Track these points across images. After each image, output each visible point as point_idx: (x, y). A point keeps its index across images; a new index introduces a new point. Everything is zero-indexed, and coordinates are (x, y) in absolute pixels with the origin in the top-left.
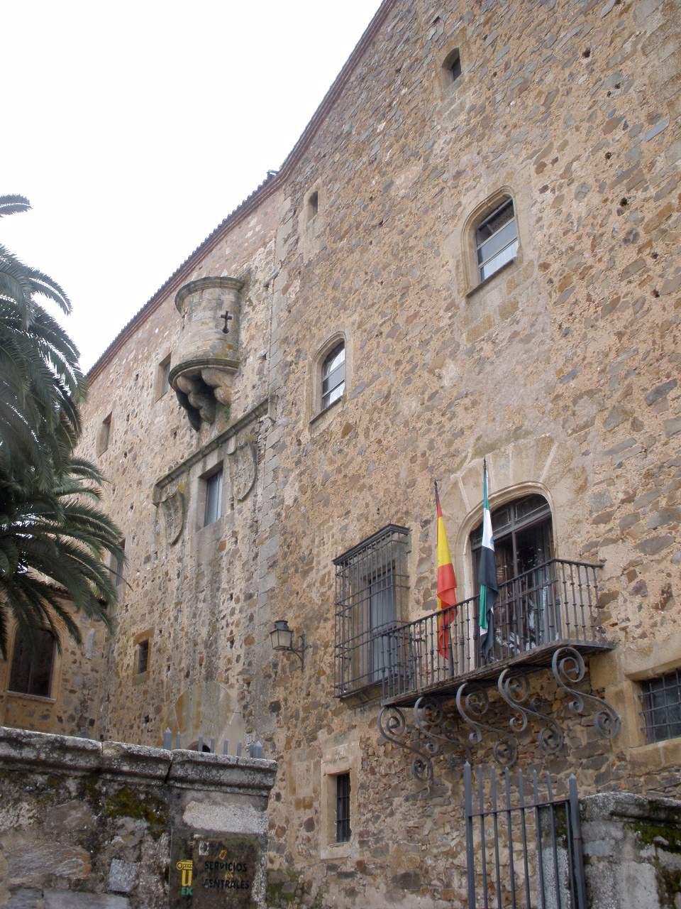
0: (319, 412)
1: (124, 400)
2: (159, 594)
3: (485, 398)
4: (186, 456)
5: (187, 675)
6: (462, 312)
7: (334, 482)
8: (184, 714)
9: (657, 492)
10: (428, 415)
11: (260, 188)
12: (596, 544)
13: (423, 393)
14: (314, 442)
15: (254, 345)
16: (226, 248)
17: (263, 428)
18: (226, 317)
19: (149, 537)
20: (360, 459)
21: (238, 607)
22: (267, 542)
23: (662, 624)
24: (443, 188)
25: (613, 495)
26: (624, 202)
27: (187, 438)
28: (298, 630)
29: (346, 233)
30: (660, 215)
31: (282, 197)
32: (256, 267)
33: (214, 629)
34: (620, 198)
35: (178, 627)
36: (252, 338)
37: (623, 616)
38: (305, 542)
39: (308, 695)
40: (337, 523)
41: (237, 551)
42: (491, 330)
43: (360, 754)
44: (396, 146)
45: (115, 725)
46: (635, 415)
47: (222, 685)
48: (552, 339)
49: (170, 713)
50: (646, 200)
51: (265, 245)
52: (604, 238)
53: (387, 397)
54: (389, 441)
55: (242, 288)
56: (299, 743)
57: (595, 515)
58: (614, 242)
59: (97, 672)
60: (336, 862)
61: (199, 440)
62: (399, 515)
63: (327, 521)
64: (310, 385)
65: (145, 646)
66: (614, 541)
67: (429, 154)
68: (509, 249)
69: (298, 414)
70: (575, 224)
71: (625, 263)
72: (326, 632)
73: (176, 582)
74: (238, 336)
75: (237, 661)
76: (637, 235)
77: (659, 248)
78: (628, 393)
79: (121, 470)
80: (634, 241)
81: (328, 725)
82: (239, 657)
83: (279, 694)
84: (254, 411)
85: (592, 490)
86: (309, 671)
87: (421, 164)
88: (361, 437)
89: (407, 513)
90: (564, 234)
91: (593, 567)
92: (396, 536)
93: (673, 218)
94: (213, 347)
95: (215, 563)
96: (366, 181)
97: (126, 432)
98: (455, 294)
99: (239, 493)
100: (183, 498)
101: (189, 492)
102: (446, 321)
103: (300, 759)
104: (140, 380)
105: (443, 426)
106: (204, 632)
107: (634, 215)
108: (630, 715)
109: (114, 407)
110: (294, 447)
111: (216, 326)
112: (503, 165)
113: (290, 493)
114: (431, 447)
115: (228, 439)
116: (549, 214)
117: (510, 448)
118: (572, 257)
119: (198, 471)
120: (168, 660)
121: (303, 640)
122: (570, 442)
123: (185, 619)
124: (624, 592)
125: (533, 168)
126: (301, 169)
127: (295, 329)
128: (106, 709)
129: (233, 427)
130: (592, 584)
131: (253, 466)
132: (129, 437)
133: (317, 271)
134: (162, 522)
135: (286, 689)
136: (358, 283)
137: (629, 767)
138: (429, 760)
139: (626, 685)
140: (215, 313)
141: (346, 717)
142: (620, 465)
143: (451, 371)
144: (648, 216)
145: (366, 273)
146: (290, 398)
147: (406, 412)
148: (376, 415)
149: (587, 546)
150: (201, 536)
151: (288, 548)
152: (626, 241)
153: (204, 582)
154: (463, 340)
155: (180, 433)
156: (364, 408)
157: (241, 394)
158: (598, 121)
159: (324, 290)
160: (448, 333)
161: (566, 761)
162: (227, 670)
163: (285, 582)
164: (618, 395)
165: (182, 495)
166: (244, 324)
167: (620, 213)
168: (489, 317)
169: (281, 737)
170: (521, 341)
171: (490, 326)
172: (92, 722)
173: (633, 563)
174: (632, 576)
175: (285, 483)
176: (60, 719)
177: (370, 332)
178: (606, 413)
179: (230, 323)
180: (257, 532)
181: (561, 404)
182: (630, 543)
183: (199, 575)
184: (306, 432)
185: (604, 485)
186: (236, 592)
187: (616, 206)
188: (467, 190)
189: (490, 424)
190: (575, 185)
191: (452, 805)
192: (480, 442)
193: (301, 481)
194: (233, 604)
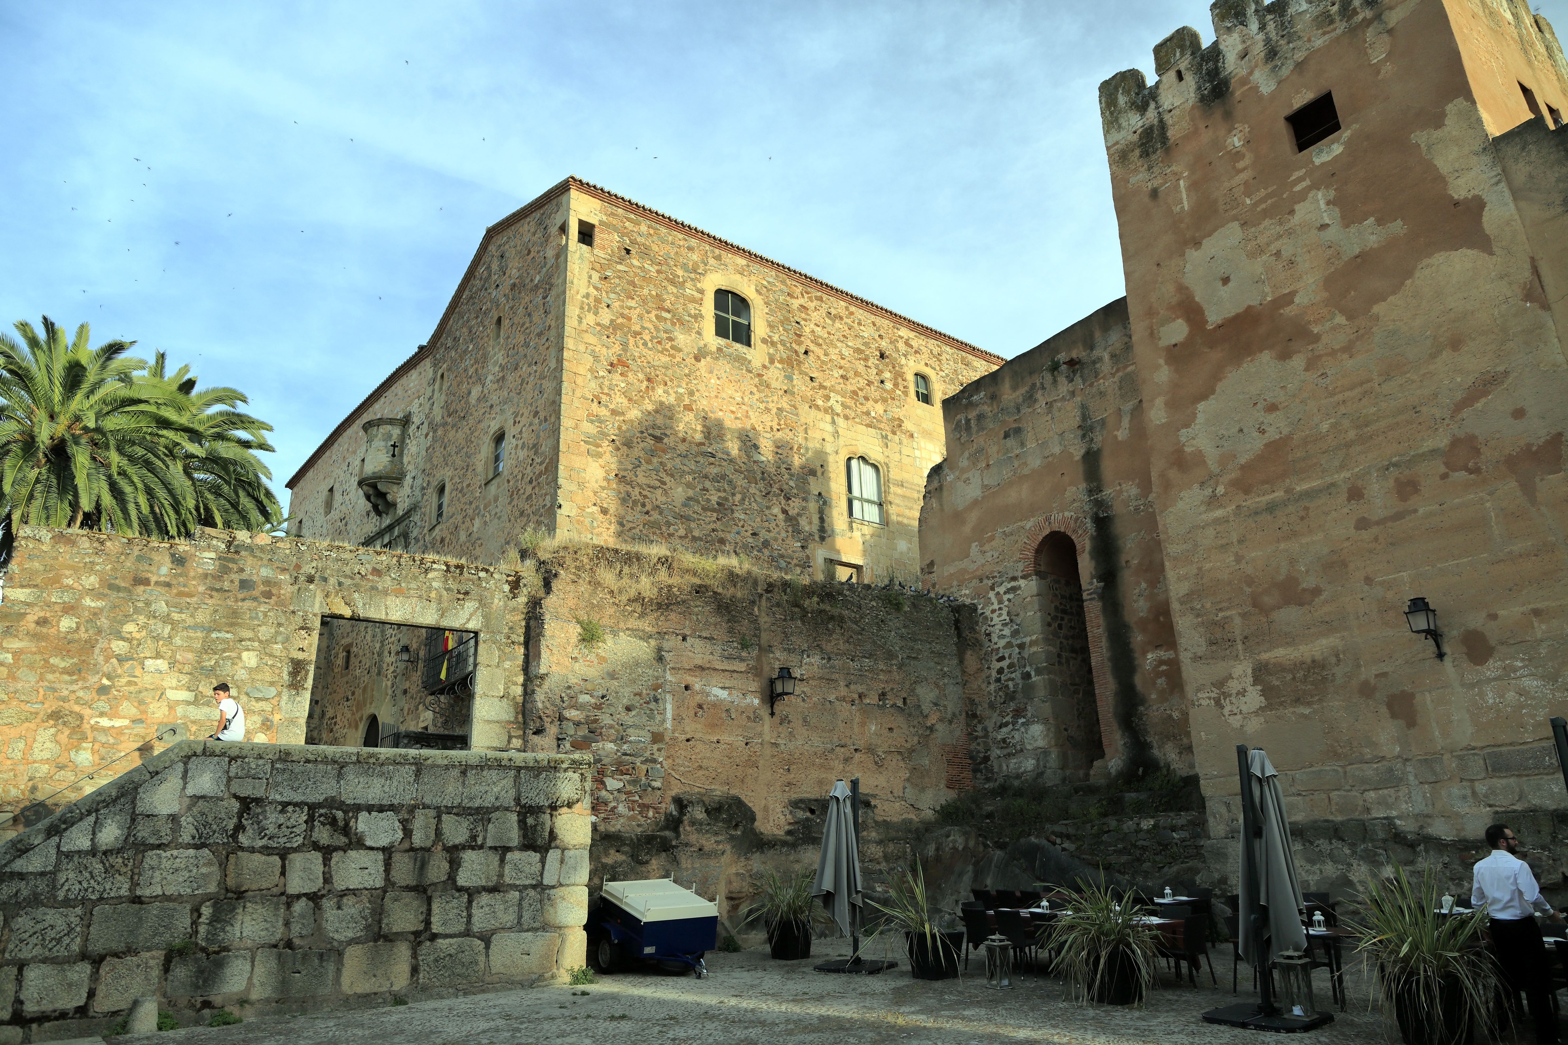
18: (394, 446)
65: (348, 652)
94: (385, 467)
106: (378, 645)
110: (422, 542)
123: (369, 638)
179: (397, 449)
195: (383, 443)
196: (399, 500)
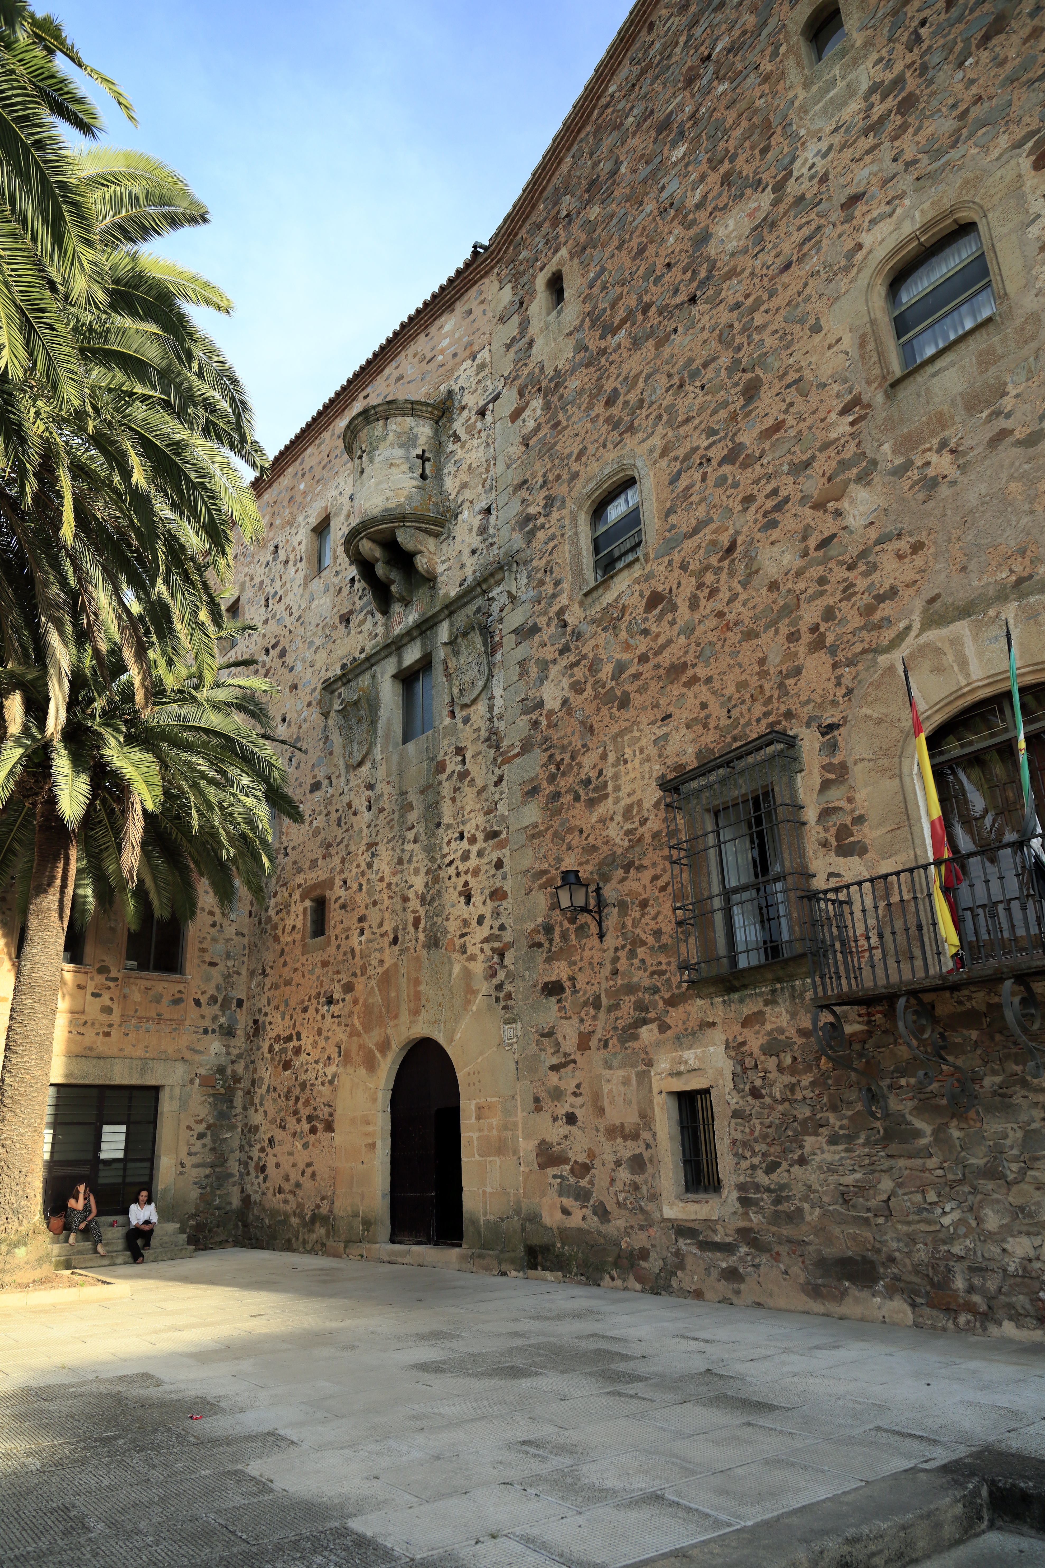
1: (257, 580)
5: (395, 941)
8: (393, 994)
13: (804, 539)
15: (468, 494)
18: (422, 457)
21: (474, 849)
22: (517, 760)
38: (588, 761)
40: (647, 734)
41: (464, 775)
47: (456, 956)
61: (387, 626)
64: (575, 541)
73: (366, 817)
86: (611, 941)
88: (683, 609)
94: (409, 498)
95: (430, 789)
100: (372, 704)
104: (282, 553)
106: (419, 882)
111: (411, 470)
113: (552, 694)
145: (669, 376)
155: (355, 620)
157: (451, 562)
162: (462, 935)
166: (450, 468)
180: (498, 747)
186: (469, 829)
188: (873, 222)
194: (465, 845)
195: (399, 452)
196: (440, 569)
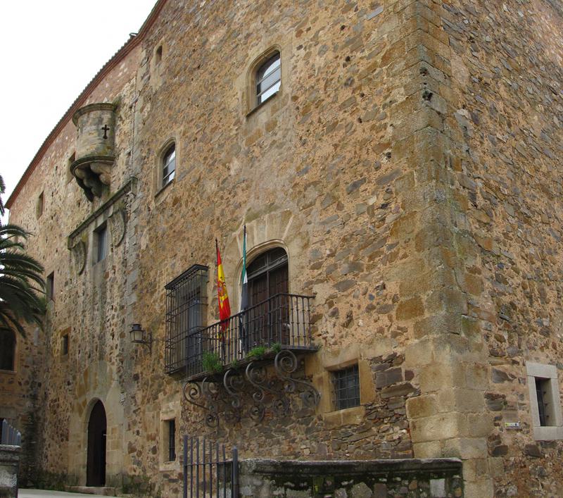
0: (161, 188)
1: (50, 183)
2: (73, 305)
3: (254, 183)
4: (86, 218)
5: (89, 357)
6: (243, 126)
7: (168, 236)
8: (88, 380)
9: (349, 251)
10: (221, 193)
11: (126, 44)
12: (311, 283)
13: (219, 179)
14: (157, 209)
15: (124, 146)
16: (105, 84)
17: (129, 199)
18: (105, 129)
19: (67, 270)
20: (183, 220)
21: (116, 314)
22: (132, 273)
23: (346, 337)
24: (238, 45)
25: (323, 251)
26: (348, 59)
27: (86, 207)
28: (148, 329)
29: (178, 73)
30: (368, 69)
31: (141, 49)
32: (125, 96)
33: (103, 328)
34: (346, 56)
35: (85, 326)
36: (122, 141)
37: (324, 330)
38: (152, 274)
39: (154, 370)
40: (170, 262)
41: (115, 278)
42: (259, 139)
43: (180, 408)
44: (211, 17)
45: (52, 386)
46: (340, 200)
47: (108, 363)
48: (296, 147)
49: (81, 380)
50: (361, 58)
51: (129, 81)
52: (333, 82)
53: (198, 181)
54: (199, 209)
55: (115, 109)
56: (148, 400)
57: (312, 263)
58: (339, 85)
59: (41, 354)
60: (168, 473)
61: (93, 207)
62: (203, 258)
63: (164, 260)
64: (155, 172)
65: (66, 338)
66: (322, 281)
67: (231, 22)
68: (273, 88)
69: (148, 191)
70: (316, 71)
71: (344, 99)
72: (162, 331)
73: (82, 298)
74: (114, 140)
75: (116, 348)
76: (353, 81)
77: (365, 91)
78: (337, 185)
79: (50, 227)
80: (351, 85)
81: (164, 390)
82: (117, 345)
83: (138, 370)
84: (123, 189)
85: (312, 247)
86: (154, 356)
87: (226, 28)
88: (184, 206)
89: (208, 256)
90: (309, 78)
91: (308, 298)
92: (200, 272)
93: (377, 72)
94: (97, 149)
95: (103, 286)
96: (192, 39)
97: (52, 204)
98: (240, 114)
99: (115, 241)
100: (85, 245)
101: (88, 241)
102: (234, 132)
103: (149, 411)
104: (58, 170)
105: (230, 201)
106: (98, 329)
107: (352, 68)
108: (325, 393)
109: (45, 187)
110: (146, 212)
111: (99, 135)
112: (276, 30)
113: (144, 242)
114: (222, 215)
115: (110, 206)
116: (301, 64)
117: (266, 217)
118: (312, 93)
119: (92, 227)
120: (79, 347)
121: (151, 335)
122: (301, 215)
123: (87, 322)
124: (326, 315)
125: (294, 33)
126: (152, 31)
127: (147, 136)
128: (47, 377)
129: (112, 199)
130: (307, 309)
131: (123, 225)
132: (54, 206)
133: (161, 98)
134: (74, 260)
135: (142, 366)
136: (184, 106)
137: (324, 425)
138: (217, 414)
139: (324, 374)
140: (98, 127)
141: (173, 385)
142: (329, 232)
143: (235, 164)
144: (362, 69)
145: (189, 99)
146: (144, 180)
147: (209, 191)
148: (192, 192)
149: (306, 283)
150: (95, 269)
151: (143, 276)
152: (346, 84)
153: (97, 298)
154: (243, 144)
155: (82, 203)
156: (185, 187)
157: (117, 177)
158: (339, 5)
159: (164, 110)
160: (235, 141)
161: (290, 419)
162: (111, 353)
163: (142, 298)
164: (330, 186)
165: (84, 244)
166: (118, 133)
167: (345, 65)
168: (259, 130)
169: (139, 396)
170: (277, 146)
171: (260, 136)
172: (40, 385)
173: (332, 297)
174: (331, 305)
175: (141, 235)
176: (20, 383)
177: (190, 138)
178: (323, 197)
179: (108, 133)
180: (126, 266)
181: (298, 190)
182: (331, 283)
183: (95, 294)
184: (153, 203)
185: (318, 244)
186: (115, 304)
187: (343, 61)
188: (252, 46)
189: (256, 200)
190: (320, 45)
191: (229, 443)
192: (250, 212)
193: (150, 234)
194: (113, 312)
195: (94, 127)
196: (112, 180)
